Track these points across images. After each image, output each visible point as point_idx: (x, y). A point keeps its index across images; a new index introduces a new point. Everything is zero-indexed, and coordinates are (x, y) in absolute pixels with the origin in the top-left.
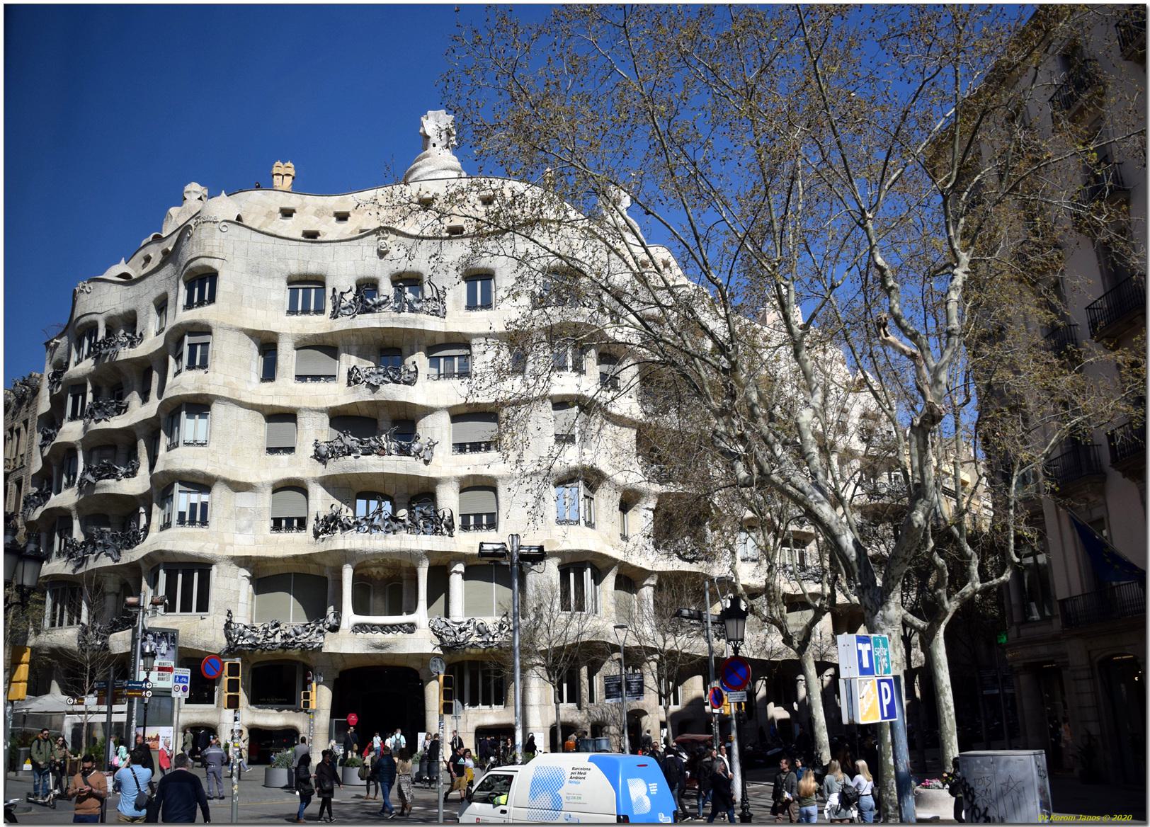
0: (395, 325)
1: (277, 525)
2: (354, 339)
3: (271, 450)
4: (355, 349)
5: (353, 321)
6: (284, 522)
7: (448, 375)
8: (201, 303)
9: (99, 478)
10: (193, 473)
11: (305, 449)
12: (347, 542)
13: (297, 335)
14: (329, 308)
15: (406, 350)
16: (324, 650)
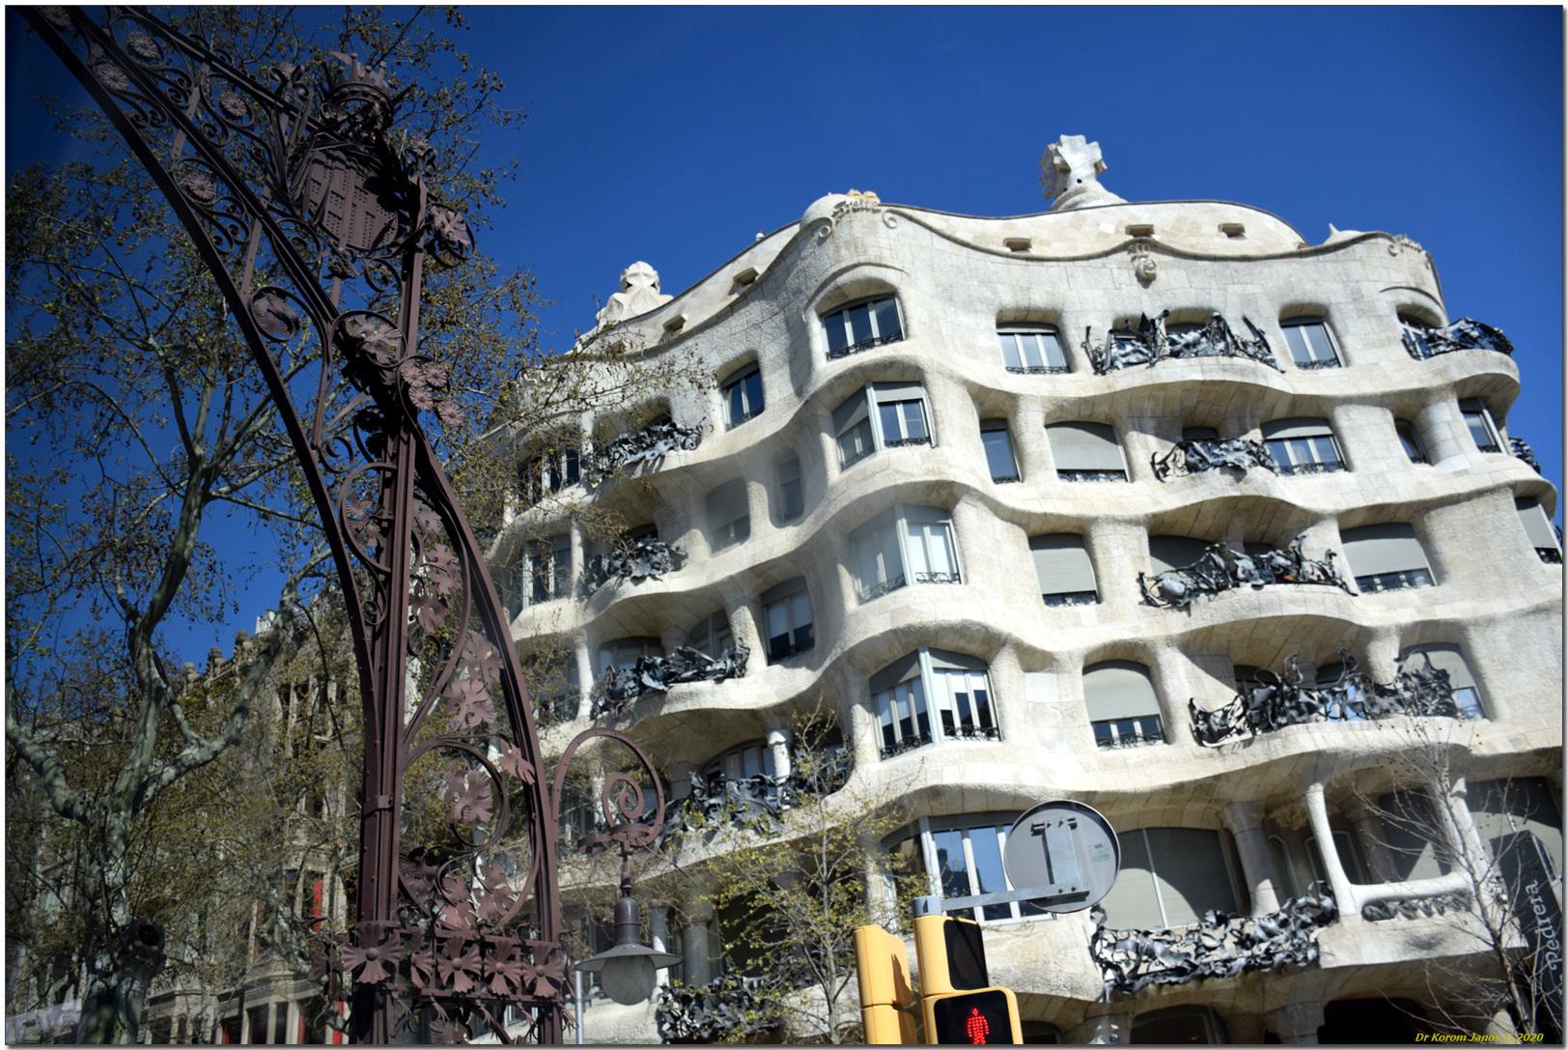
0: (1229, 377)
1: (1102, 732)
2: (1148, 405)
3: (1051, 599)
4: (1150, 424)
5: (1153, 371)
6: (1114, 729)
7: (1310, 467)
8: (864, 342)
9: (670, 678)
10: (962, 630)
11: (1122, 589)
12: (1317, 736)
13: (1051, 399)
14: (1083, 361)
15: (1232, 427)
16: (1326, 963)
